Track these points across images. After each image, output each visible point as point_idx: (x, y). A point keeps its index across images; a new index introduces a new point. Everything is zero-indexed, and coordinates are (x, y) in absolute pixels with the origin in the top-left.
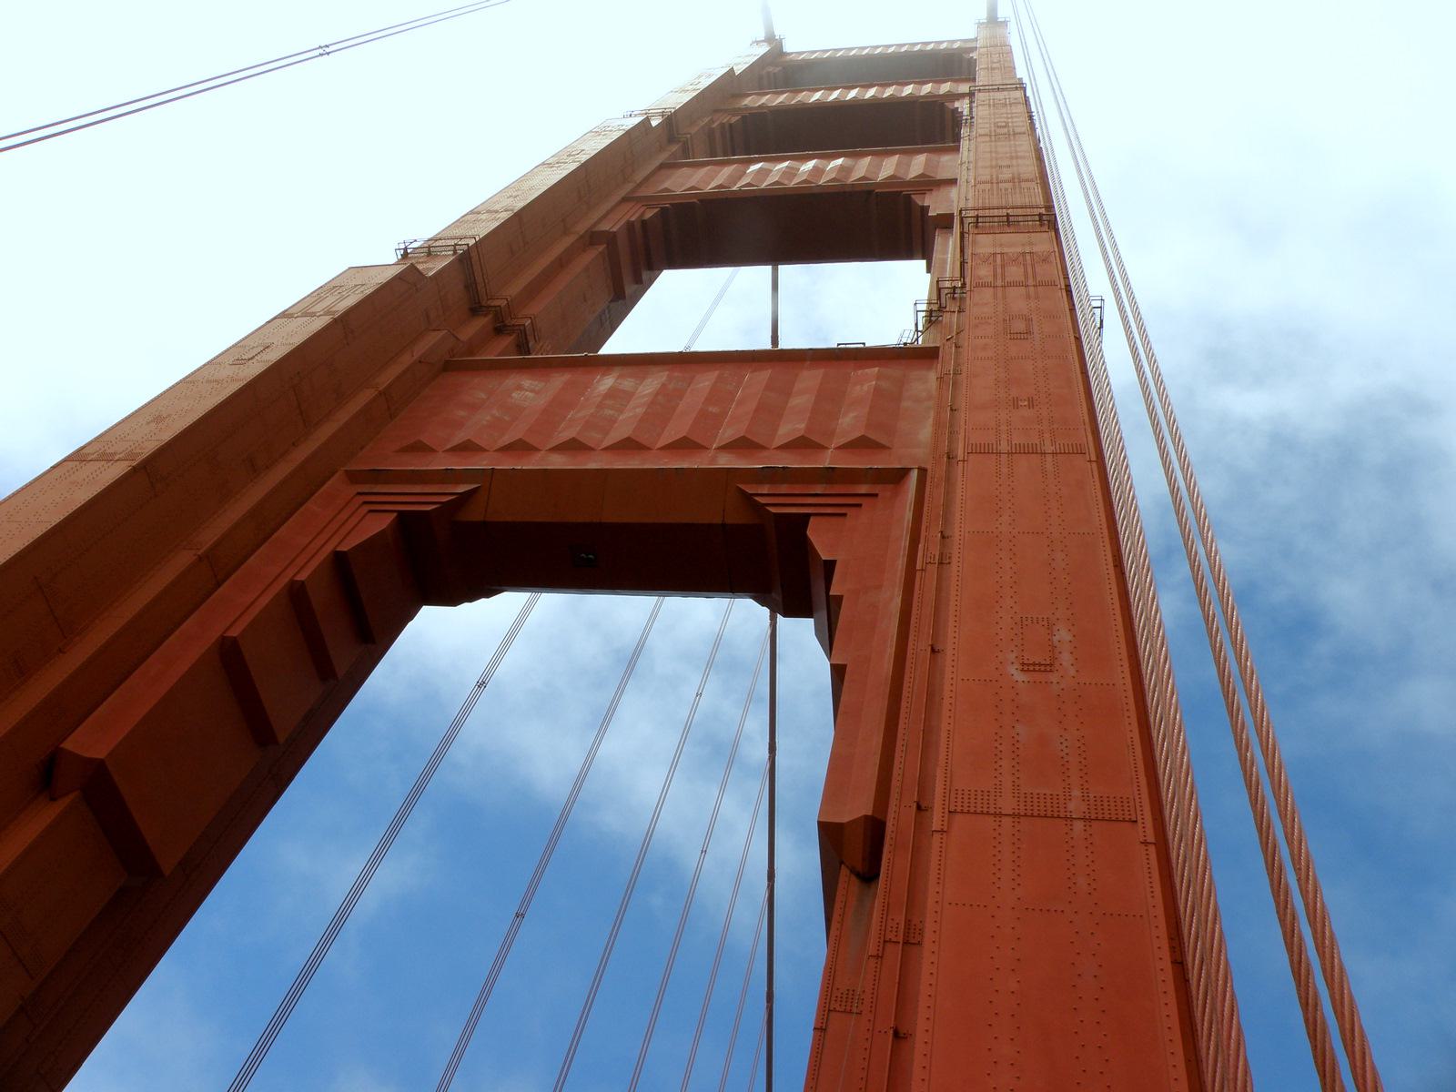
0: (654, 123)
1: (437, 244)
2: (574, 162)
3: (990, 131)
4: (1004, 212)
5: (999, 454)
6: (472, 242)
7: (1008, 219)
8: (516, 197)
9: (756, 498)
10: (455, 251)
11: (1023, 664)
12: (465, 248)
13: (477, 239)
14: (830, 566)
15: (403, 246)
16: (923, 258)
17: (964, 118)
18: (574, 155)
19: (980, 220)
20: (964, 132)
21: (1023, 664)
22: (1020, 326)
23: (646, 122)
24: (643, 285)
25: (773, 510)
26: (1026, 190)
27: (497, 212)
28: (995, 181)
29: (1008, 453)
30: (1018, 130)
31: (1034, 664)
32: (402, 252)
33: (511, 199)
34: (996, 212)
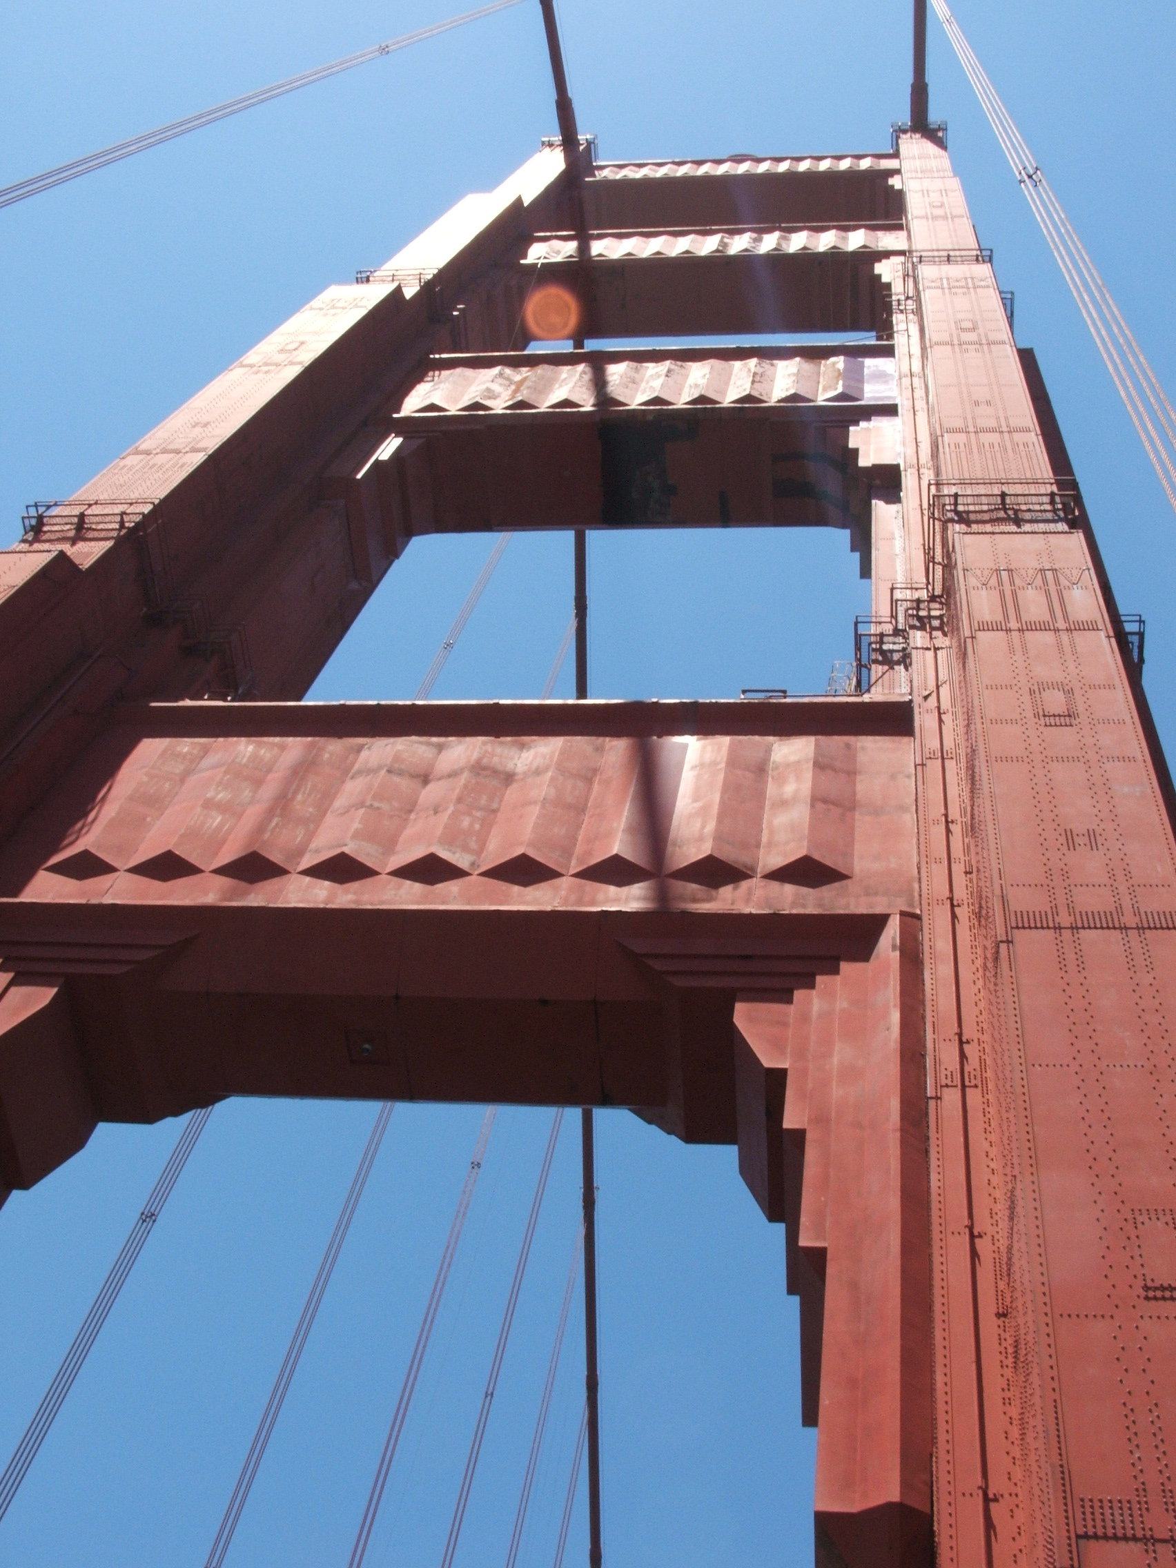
0: (409, 293)
1: (96, 510)
2: (292, 363)
3: (951, 335)
4: (996, 490)
5: (1058, 928)
6: (147, 509)
7: (1003, 502)
8: (205, 425)
9: (650, 962)
10: (122, 523)
11: (1146, 1288)
12: (138, 518)
13: (157, 502)
14: (778, 1078)
15: (33, 512)
16: (844, 527)
17: (894, 298)
18: (290, 351)
19: (960, 500)
20: (898, 320)
21: (1146, 1288)
22: (1055, 701)
23: (398, 291)
24: (392, 552)
25: (679, 982)
26: (1021, 447)
27: (177, 452)
28: (971, 429)
29: (1072, 928)
30: (992, 337)
31: (1162, 1288)
32: (34, 522)
33: (198, 430)
34: (982, 490)
